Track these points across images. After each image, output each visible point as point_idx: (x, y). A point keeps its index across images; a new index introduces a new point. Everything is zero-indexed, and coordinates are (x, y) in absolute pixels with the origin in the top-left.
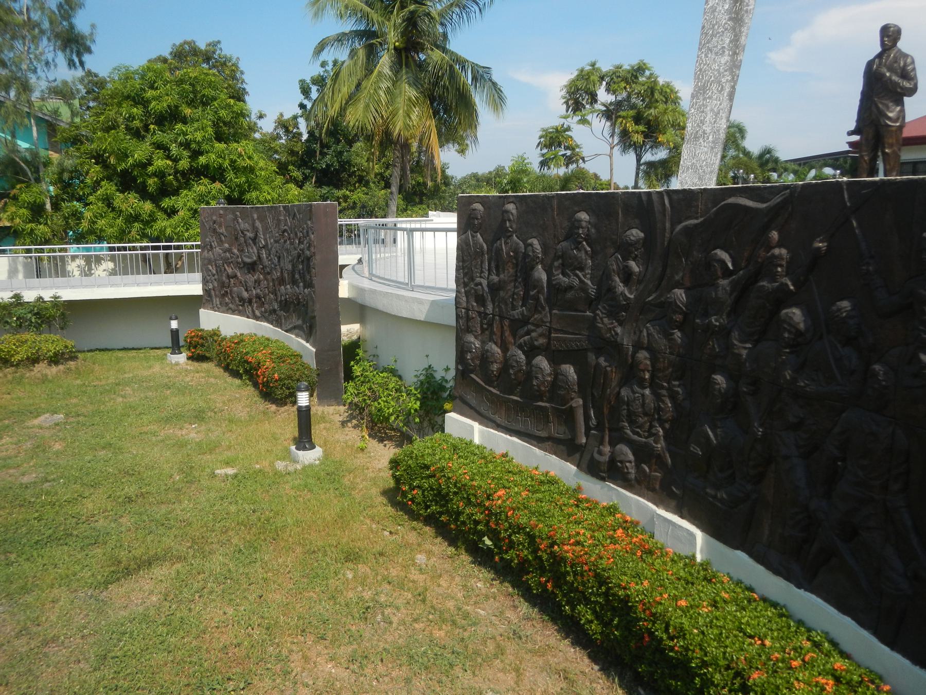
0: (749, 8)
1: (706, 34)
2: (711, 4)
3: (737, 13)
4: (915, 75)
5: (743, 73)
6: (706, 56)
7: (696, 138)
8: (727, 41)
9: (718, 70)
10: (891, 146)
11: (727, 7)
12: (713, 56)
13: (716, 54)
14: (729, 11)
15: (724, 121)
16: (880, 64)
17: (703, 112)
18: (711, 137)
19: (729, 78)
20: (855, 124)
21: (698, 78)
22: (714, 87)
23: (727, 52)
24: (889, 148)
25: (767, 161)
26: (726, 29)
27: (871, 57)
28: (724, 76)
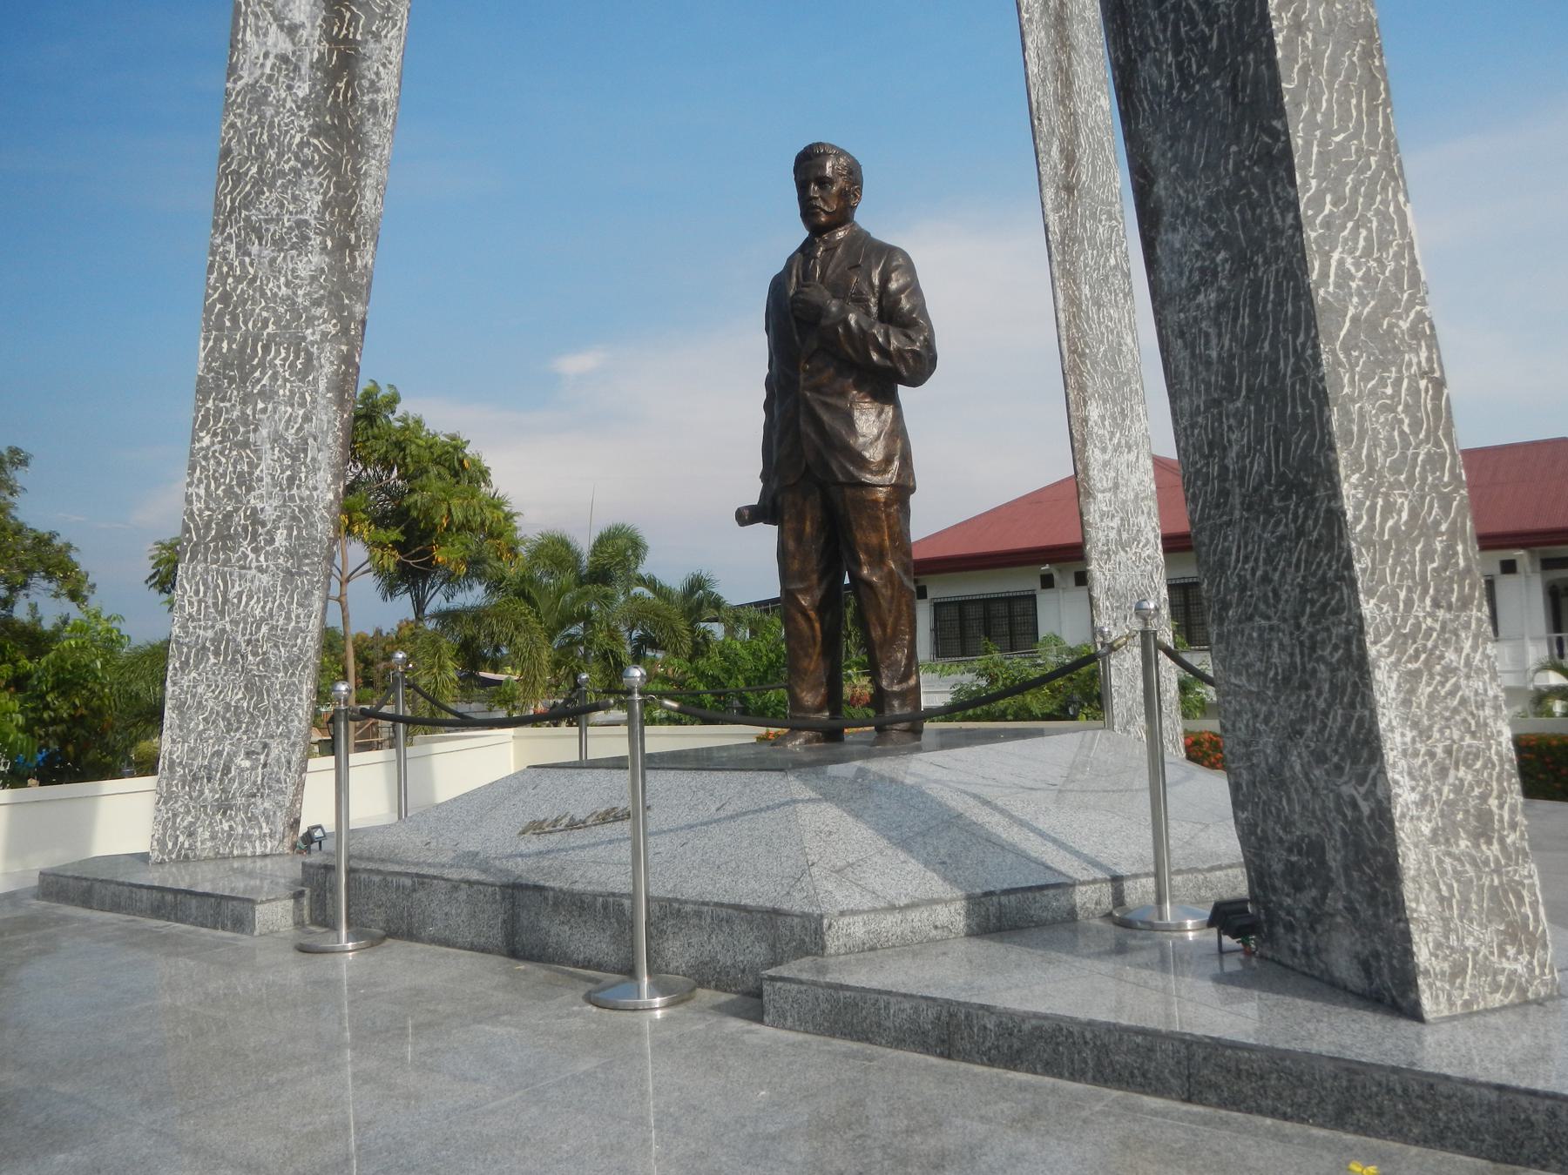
0: (380, 98)
1: (238, 177)
2: (246, 79)
3: (340, 112)
4: (924, 313)
5: (378, 310)
6: (243, 250)
7: (226, 539)
8: (314, 202)
9: (291, 302)
10: (878, 558)
11: (303, 89)
12: (268, 253)
13: (279, 243)
14: (310, 105)
15: (325, 476)
16: (806, 275)
17: (245, 444)
18: (280, 537)
19: (331, 329)
20: (759, 485)
21: (220, 328)
22: (279, 356)
23: (316, 241)
24: (870, 565)
25: (700, 603)
26: (306, 164)
27: (779, 267)
28: (310, 321)
